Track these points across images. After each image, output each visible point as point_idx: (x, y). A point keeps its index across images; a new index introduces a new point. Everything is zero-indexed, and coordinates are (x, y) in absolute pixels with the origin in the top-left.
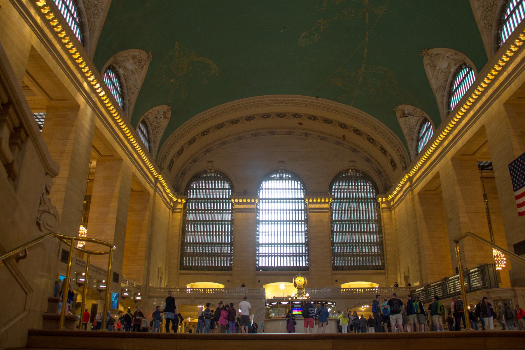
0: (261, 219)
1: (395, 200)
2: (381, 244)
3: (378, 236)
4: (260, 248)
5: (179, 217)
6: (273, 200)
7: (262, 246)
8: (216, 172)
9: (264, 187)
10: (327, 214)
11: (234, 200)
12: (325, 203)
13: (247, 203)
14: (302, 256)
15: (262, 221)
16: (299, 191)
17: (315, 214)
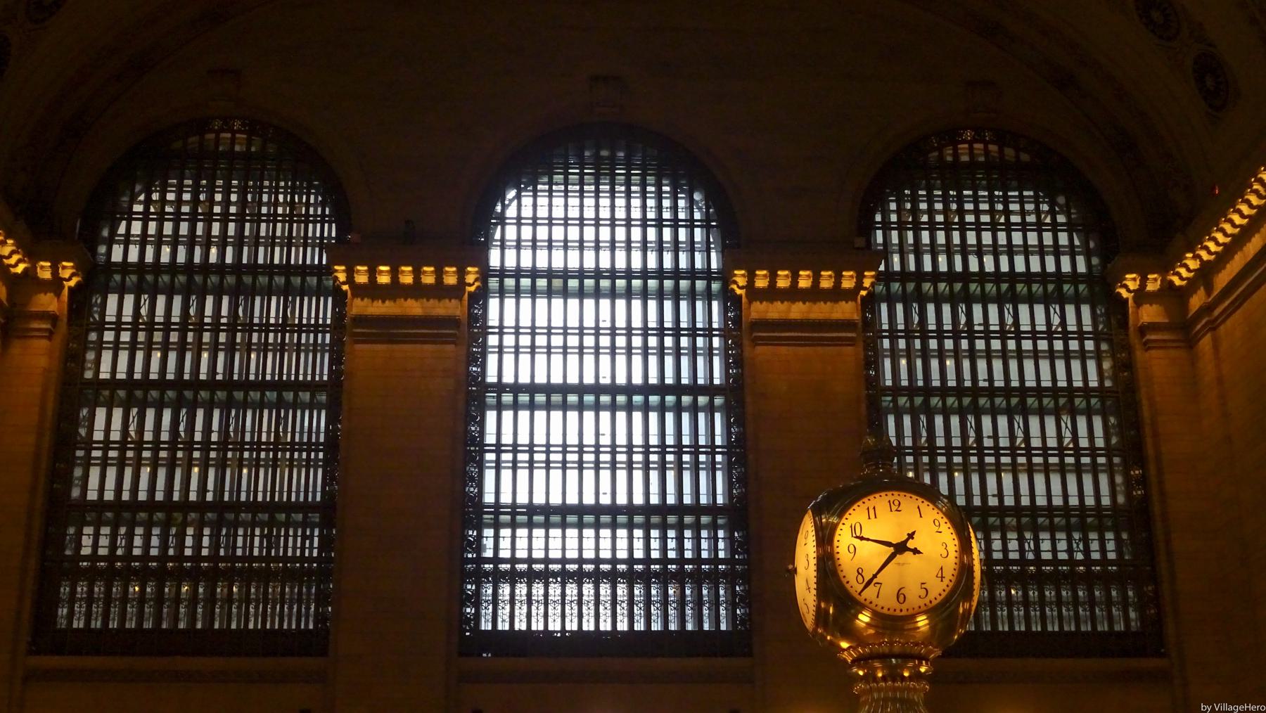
0: (492, 378)
1: (1222, 279)
2: (1136, 518)
3: (1119, 479)
4: (489, 532)
5: (43, 362)
6: (558, 283)
7: (497, 526)
8: (253, 128)
9: (511, 212)
10: (851, 355)
11: (350, 273)
12: (836, 294)
13: (417, 290)
14: (714, 578)
15: (500, 387)
16: (698, 233)
17: (783, 350)
